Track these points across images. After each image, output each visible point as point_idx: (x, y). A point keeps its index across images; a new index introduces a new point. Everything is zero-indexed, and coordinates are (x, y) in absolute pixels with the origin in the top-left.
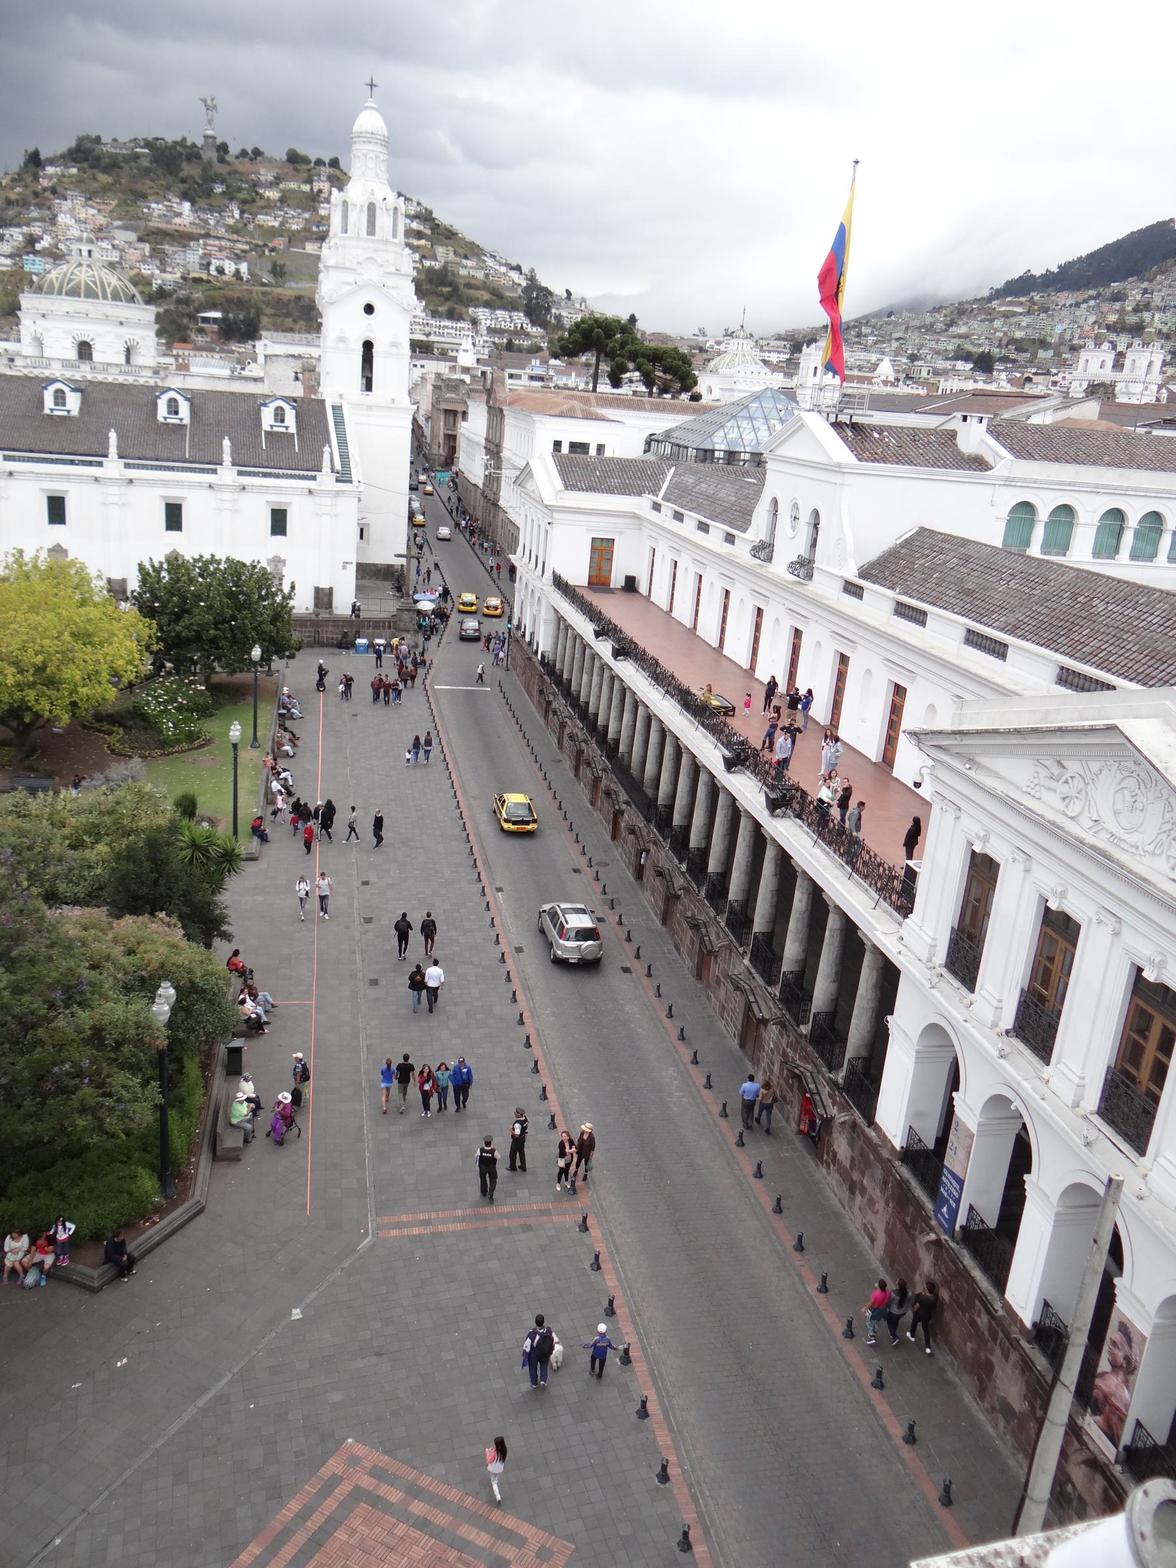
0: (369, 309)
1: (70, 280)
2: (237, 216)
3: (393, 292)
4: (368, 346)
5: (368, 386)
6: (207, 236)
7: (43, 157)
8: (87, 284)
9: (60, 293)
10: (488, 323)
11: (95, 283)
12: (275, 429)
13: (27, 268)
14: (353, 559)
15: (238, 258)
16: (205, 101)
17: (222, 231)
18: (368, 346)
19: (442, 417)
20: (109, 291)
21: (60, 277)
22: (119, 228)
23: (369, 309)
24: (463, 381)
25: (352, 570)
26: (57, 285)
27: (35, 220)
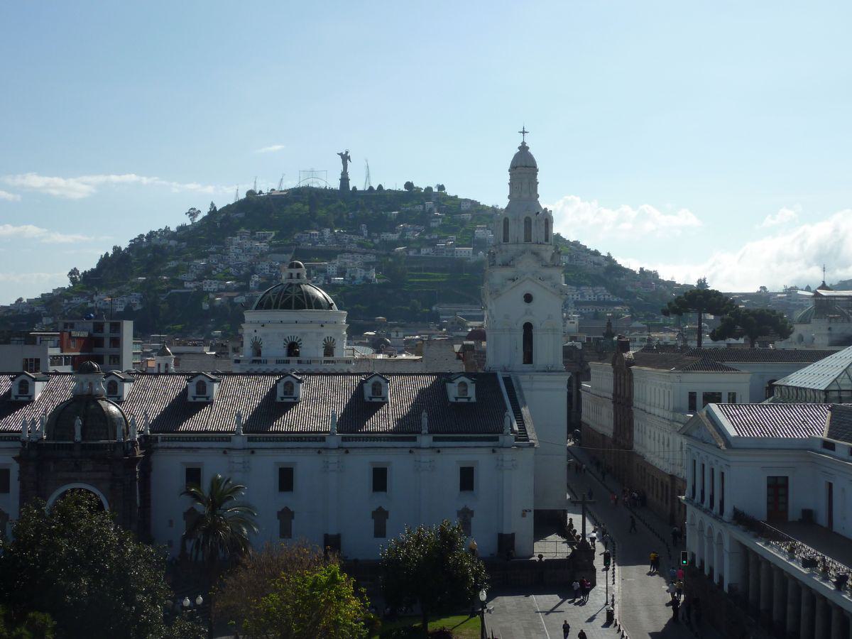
0: (528, 298)
1: (284, 297)
2: (366, 235)
4: (528, 328)
5: (528, 358)
6: (343, 252)
7: (218, 209)
8: (296, 299)
9: (276, 307)
10: (575, 297)
11: (303, 297)
12: (460, 400)
13: (206, 288)
14: (531, 507)
15: (367, 266)
16: (341, 154)
17: (354, 247)
18: (528, 328)
20: (313, 302)
22: (274, 252)
23: (528, 298)
24: (574, 347)
25: (531, 516)
26: (273, 301)
27: (212, 253)
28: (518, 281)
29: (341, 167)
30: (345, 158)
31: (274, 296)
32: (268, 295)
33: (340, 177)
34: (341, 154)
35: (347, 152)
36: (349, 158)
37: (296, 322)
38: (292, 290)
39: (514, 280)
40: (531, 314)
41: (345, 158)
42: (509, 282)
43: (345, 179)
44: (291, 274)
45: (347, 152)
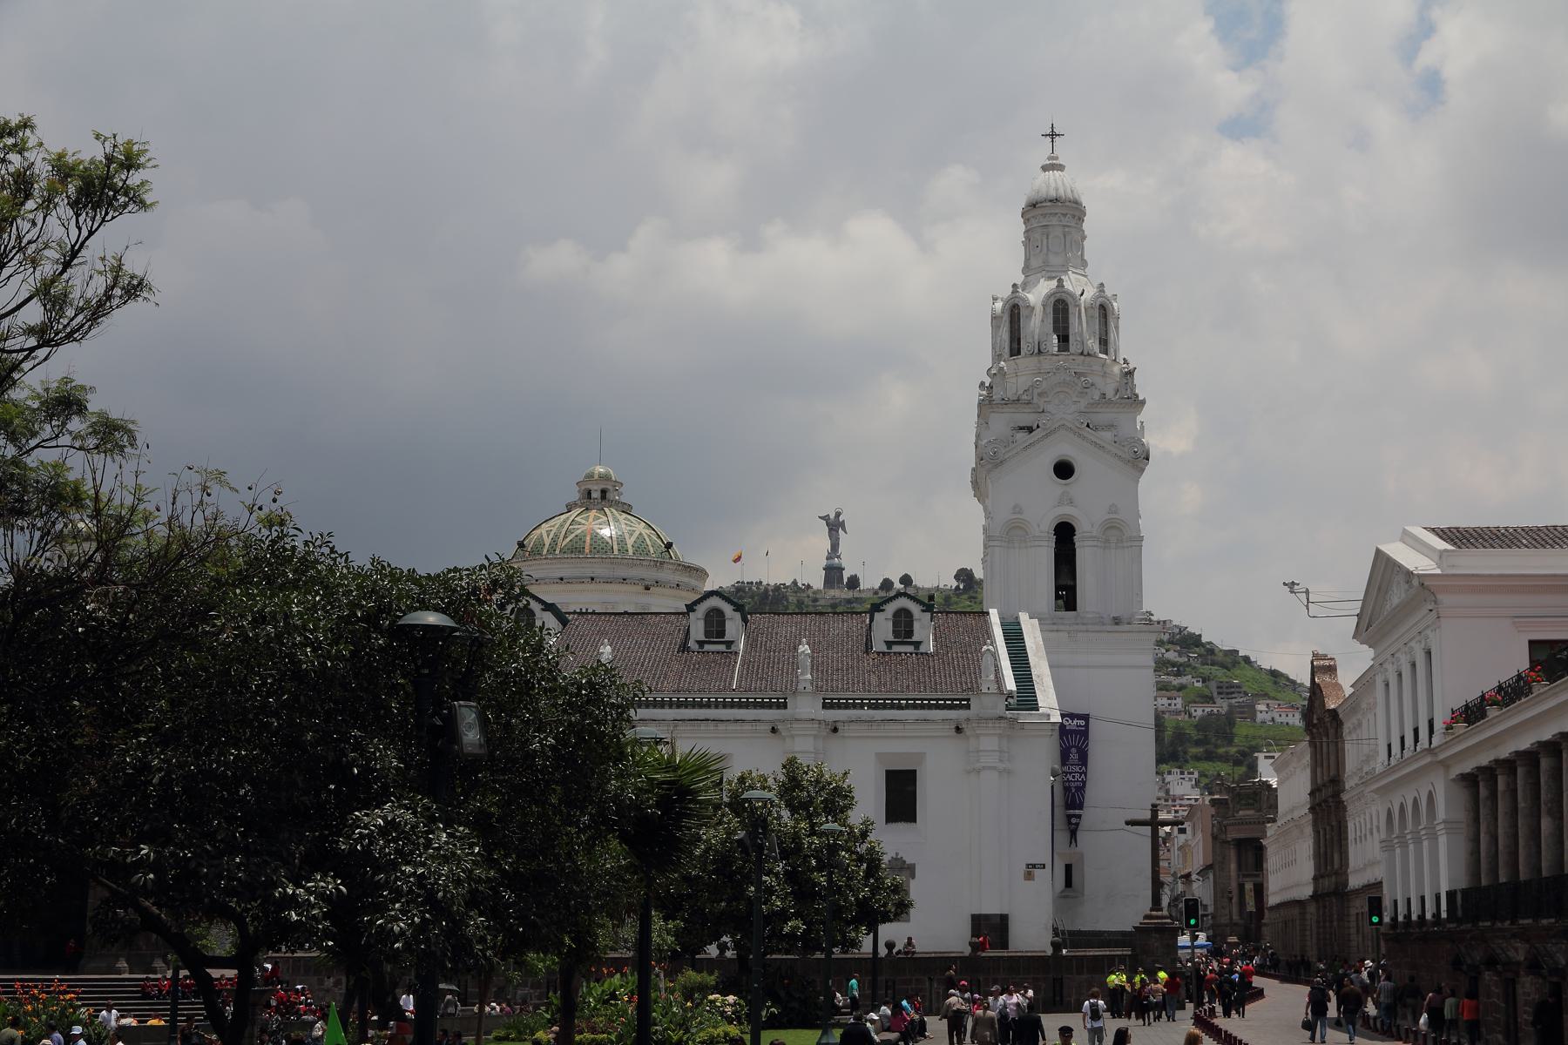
0: (1064, 470)
3: (1108, 435)
4: (1065, 534)
16: (826, 518)
18: (1065, 534)
19: (1232, 854)
21: (554, 530)
23: (1064, 470)
26: (547, 541)
28: (1037, 434)
29: (826, 544)
30: (835, 526)
31: (548, 533)
32: (538, 532)
33: (824, 563)
34: (826, 518)
35: (838, 515)
36: (842, 525)
37: (592, 579)
38: (587, 519)
39: (1030, 430)
40: (1071, 502)
41: (835, 526)
42: (1021, 435)
43: (833, 573)
44: (589, 493)
45: (838, 515)
